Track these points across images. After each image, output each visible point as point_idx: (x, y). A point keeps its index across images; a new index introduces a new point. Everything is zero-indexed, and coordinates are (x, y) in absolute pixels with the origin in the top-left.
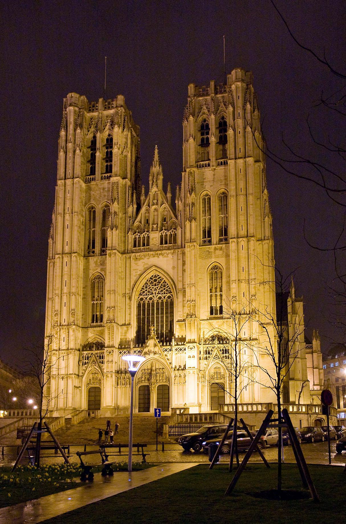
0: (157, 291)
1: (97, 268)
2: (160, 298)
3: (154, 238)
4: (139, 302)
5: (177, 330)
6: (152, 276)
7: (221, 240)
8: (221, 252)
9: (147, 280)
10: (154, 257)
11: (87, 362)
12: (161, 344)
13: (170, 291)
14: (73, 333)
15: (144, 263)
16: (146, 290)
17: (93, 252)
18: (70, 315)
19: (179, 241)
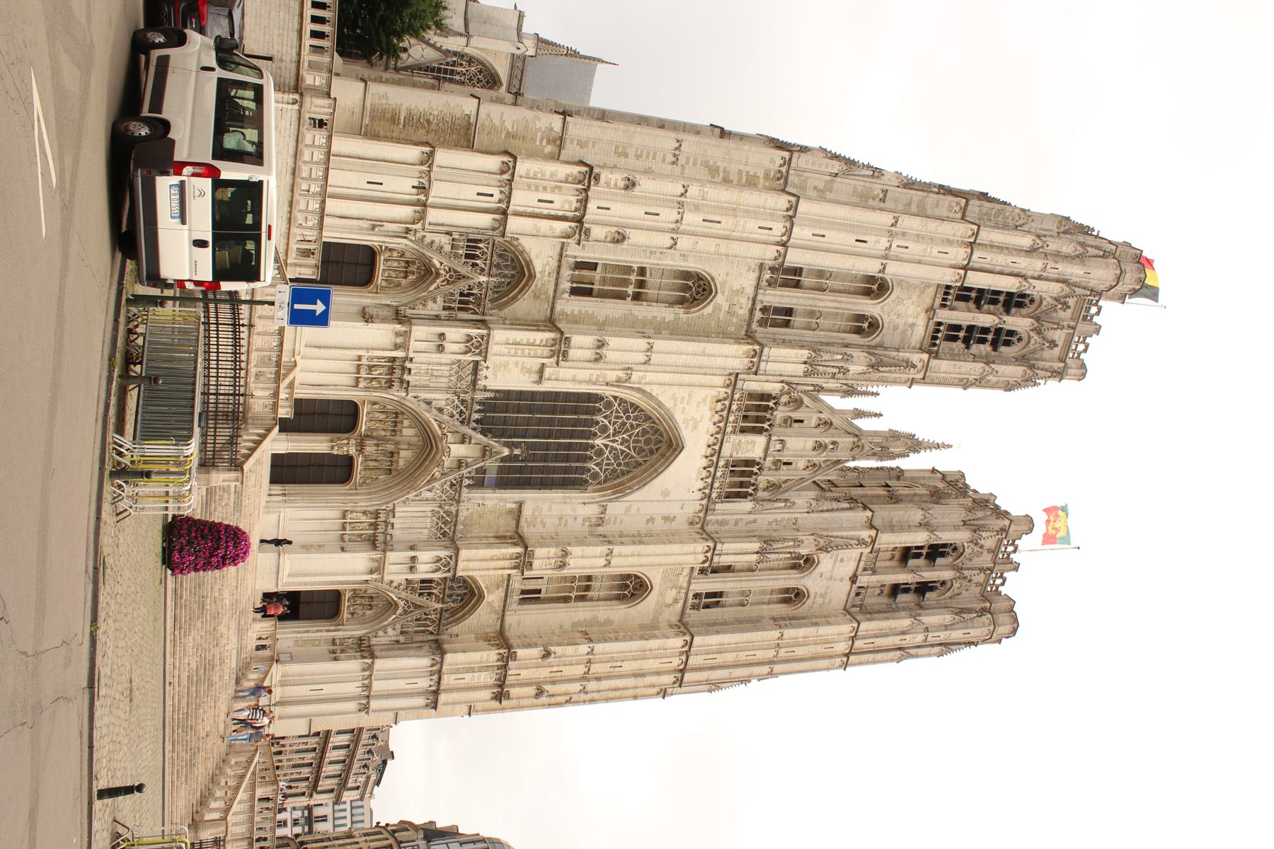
0: (619, 447)
1: (726, 294)
2: (600, 453)
3: (754, 446)
4: (602, 399)
5: (502, 504)
6: (661, 435)
7: (696, 596)
8: (669, 600)
9: (654, 422)
10: (709, 446)
11: (461, 252)
12: (473, 475)
13: (610, 479)
14: (558, 232)
15: (702, 419)
16: (628, 418)
17: (770, 284)
18: (616, 229)
19: (727, 504)
